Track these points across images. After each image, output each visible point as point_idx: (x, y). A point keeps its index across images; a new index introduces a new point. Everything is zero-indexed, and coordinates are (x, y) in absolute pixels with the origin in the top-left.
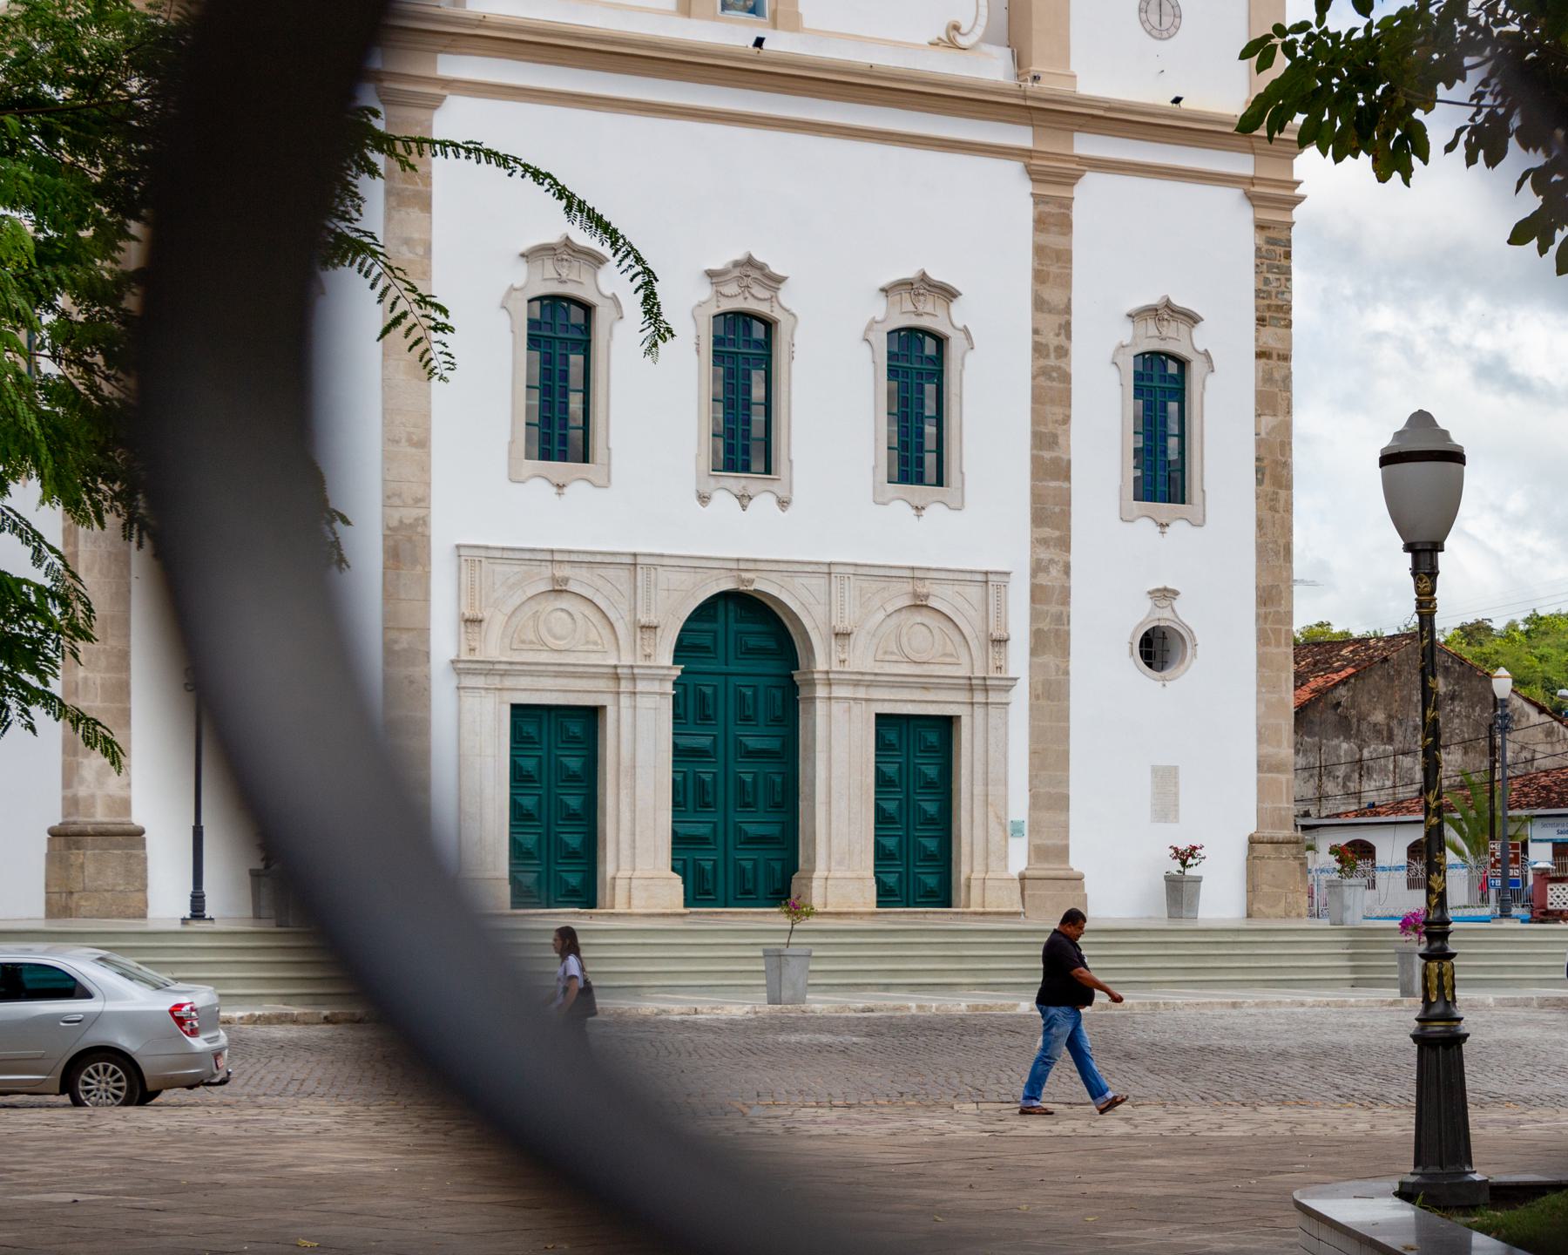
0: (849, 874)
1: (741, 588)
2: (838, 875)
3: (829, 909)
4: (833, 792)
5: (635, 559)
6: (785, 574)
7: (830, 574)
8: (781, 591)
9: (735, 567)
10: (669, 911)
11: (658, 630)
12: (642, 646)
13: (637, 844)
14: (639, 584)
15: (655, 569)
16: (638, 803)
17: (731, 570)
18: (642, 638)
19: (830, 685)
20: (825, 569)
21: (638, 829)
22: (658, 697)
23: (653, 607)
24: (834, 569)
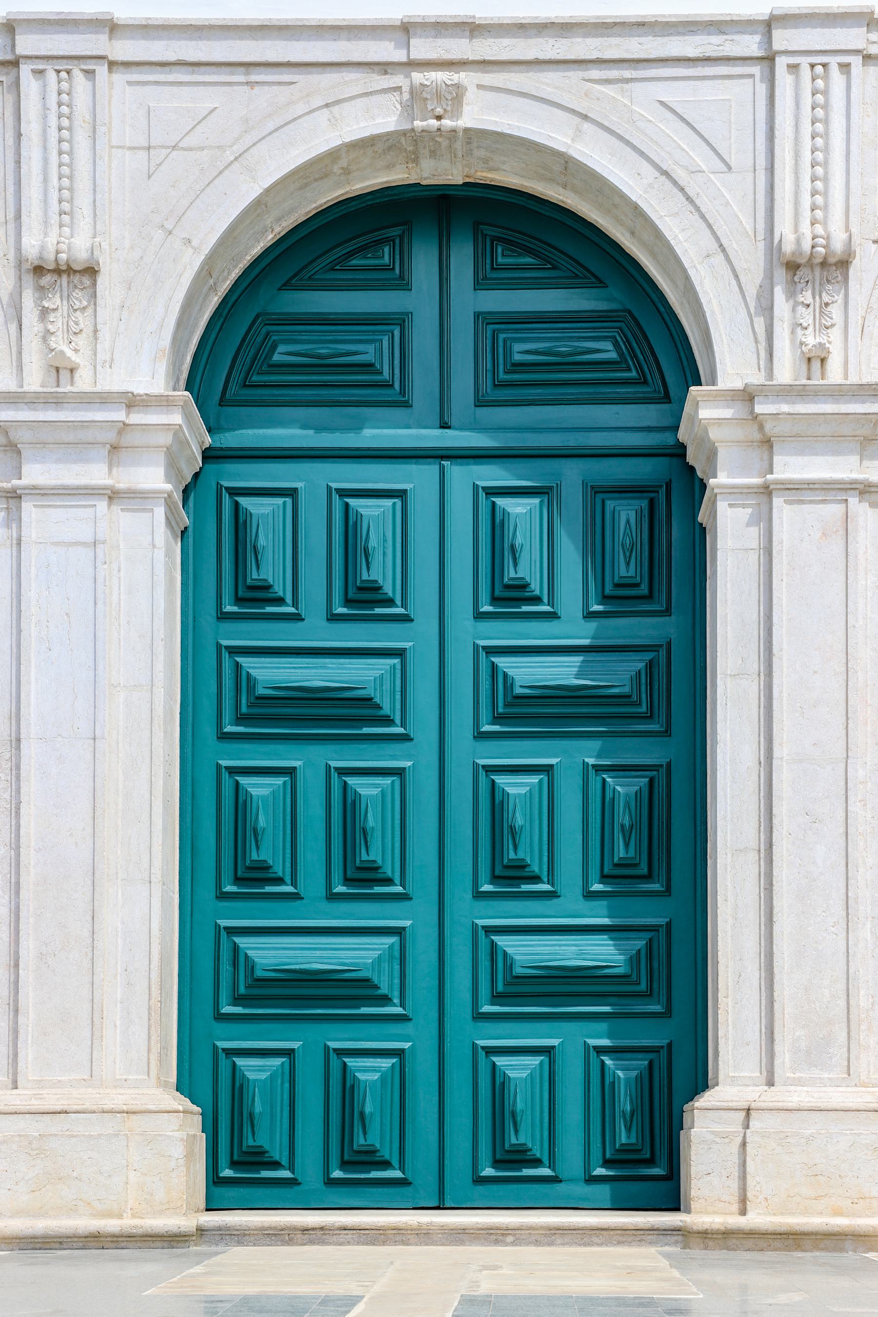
0: (838, 1096)
1: (418, 124)
2: (797, 1096)
3: (756, 1219)
4: (781, 810)
5: (13, 46)
6: (595, 73)
7: (769, 59)
8: (578, 133)
9: (400, 56)
10: (112, 1225)
11: (102, 281)
12: (47, 334)
13: (29, 996)
14: (31, 127)
15: (90, 74)
16: (29, 856)
17: (384, 67)
18: (44, 313)
19: (767, 444)
20: (751, 45)
21: (29, 947)
22: (102, 505)
23: (83, 201)
24: (782, 39)
